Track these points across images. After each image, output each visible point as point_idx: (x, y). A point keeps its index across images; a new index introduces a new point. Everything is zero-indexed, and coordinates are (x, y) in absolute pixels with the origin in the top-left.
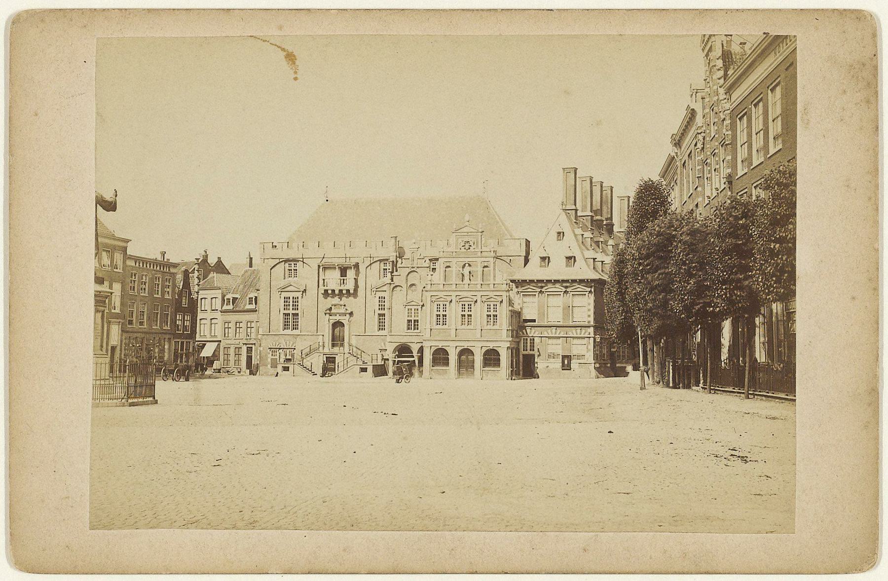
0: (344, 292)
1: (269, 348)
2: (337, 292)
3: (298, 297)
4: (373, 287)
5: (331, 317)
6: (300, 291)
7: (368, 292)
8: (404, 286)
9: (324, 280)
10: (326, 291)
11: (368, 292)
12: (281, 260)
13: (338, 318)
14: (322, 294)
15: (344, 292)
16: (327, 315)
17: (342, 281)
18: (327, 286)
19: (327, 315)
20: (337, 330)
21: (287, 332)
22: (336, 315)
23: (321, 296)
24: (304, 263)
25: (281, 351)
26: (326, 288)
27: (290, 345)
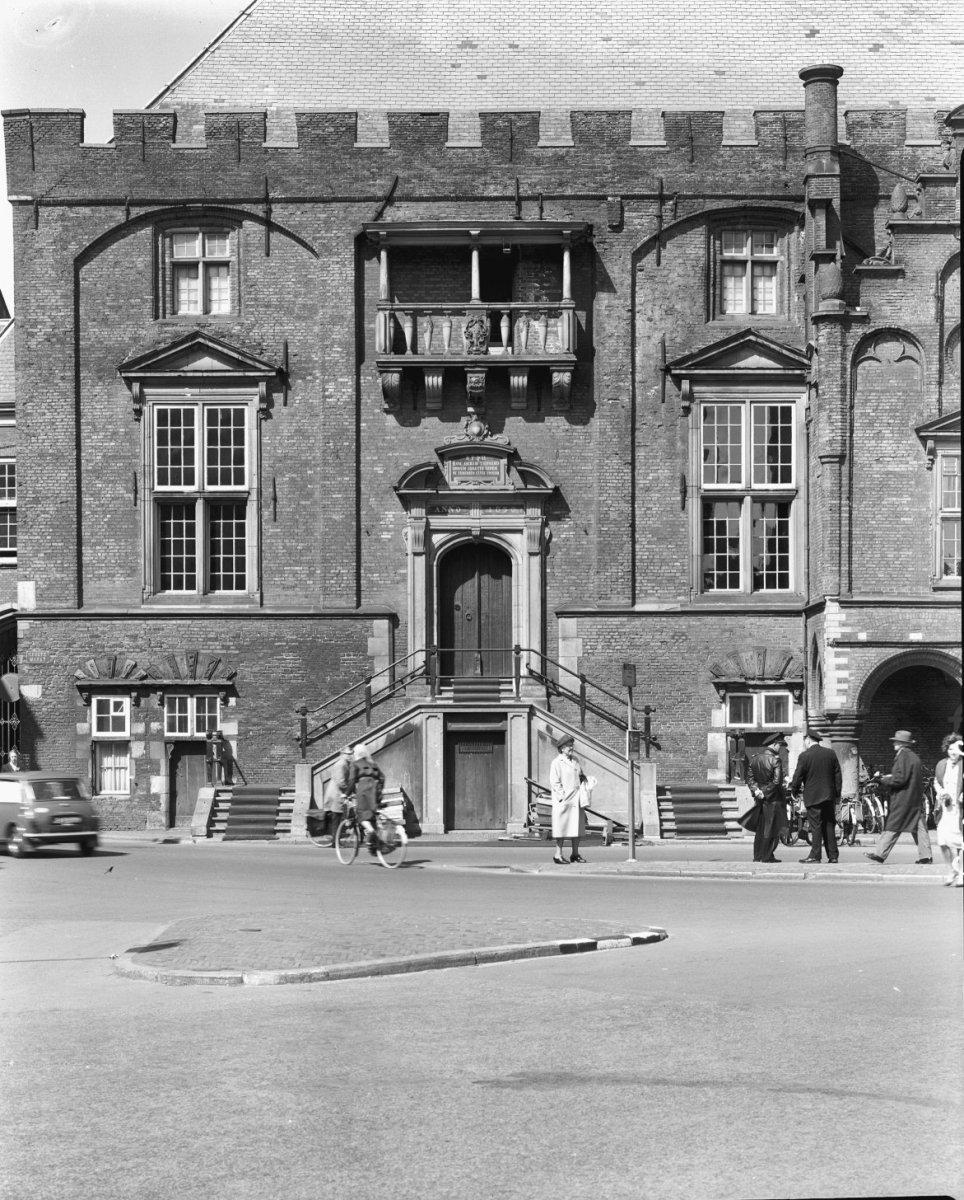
0: (519, 381)
1: (81, 689)
2: (475, 379)
3: (240, 415)
4: (669, 360)
5: (437, 522)
6: (253, 382)
10: (413, 375)
12: (136, 212)
13: (474, 520)
18: (414, 350)
20: (466, 594)
21: (178, 599)
23: (373, 401)
24: (271, 226)
26: (408, 356)
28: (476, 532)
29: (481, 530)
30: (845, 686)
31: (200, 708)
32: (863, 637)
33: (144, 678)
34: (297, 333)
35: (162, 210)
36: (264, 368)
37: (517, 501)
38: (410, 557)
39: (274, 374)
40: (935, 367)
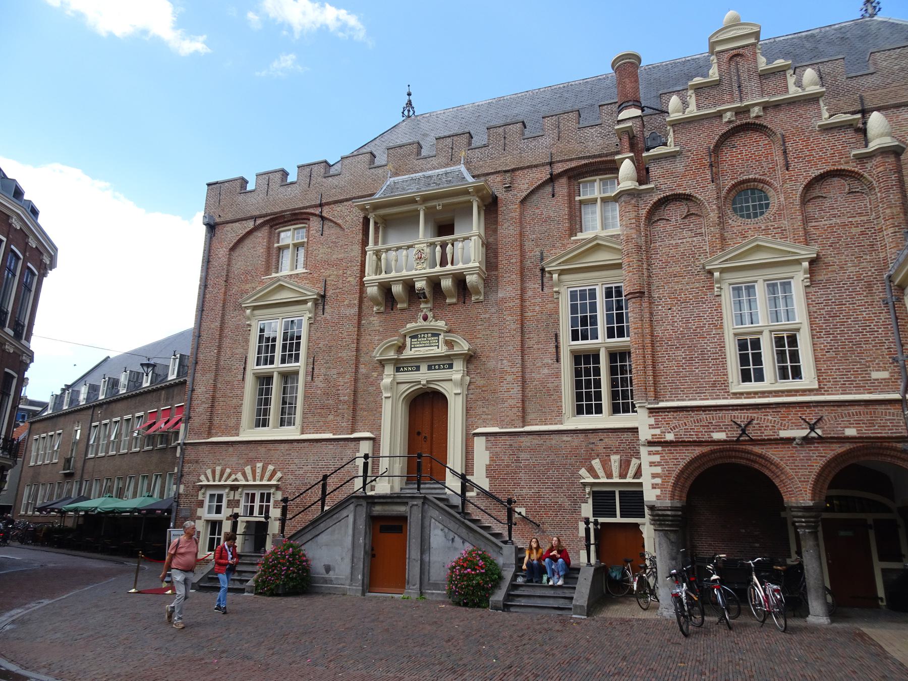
1: (202, 487)
5: (402, 376)
6: (305, 302)
7: (533, 285)
8: (706, 194)
9: (378, 254)
10: (386, 288)
11: (533, 285)
12: (259, 221)
13: (424, 376)
14: (374, 300)
15: (446, 283)
16: (389, 370)
17: (438, 248)
19: (389, 370)
22: (418, 369)
25: (239, 495)
26: (383, 275)
27: (268, 474)
28: (424, 382)
29: (427, 381)
30: (658, 481)
31: (262, 501)
32: (670, 437)
33: (236, 480)
34: (331, 273)
35: (271, 219)
36: (310, 294)
37: (446, 362)
38: (384, 399)
39: (315, 297)
40: (713, 216)
